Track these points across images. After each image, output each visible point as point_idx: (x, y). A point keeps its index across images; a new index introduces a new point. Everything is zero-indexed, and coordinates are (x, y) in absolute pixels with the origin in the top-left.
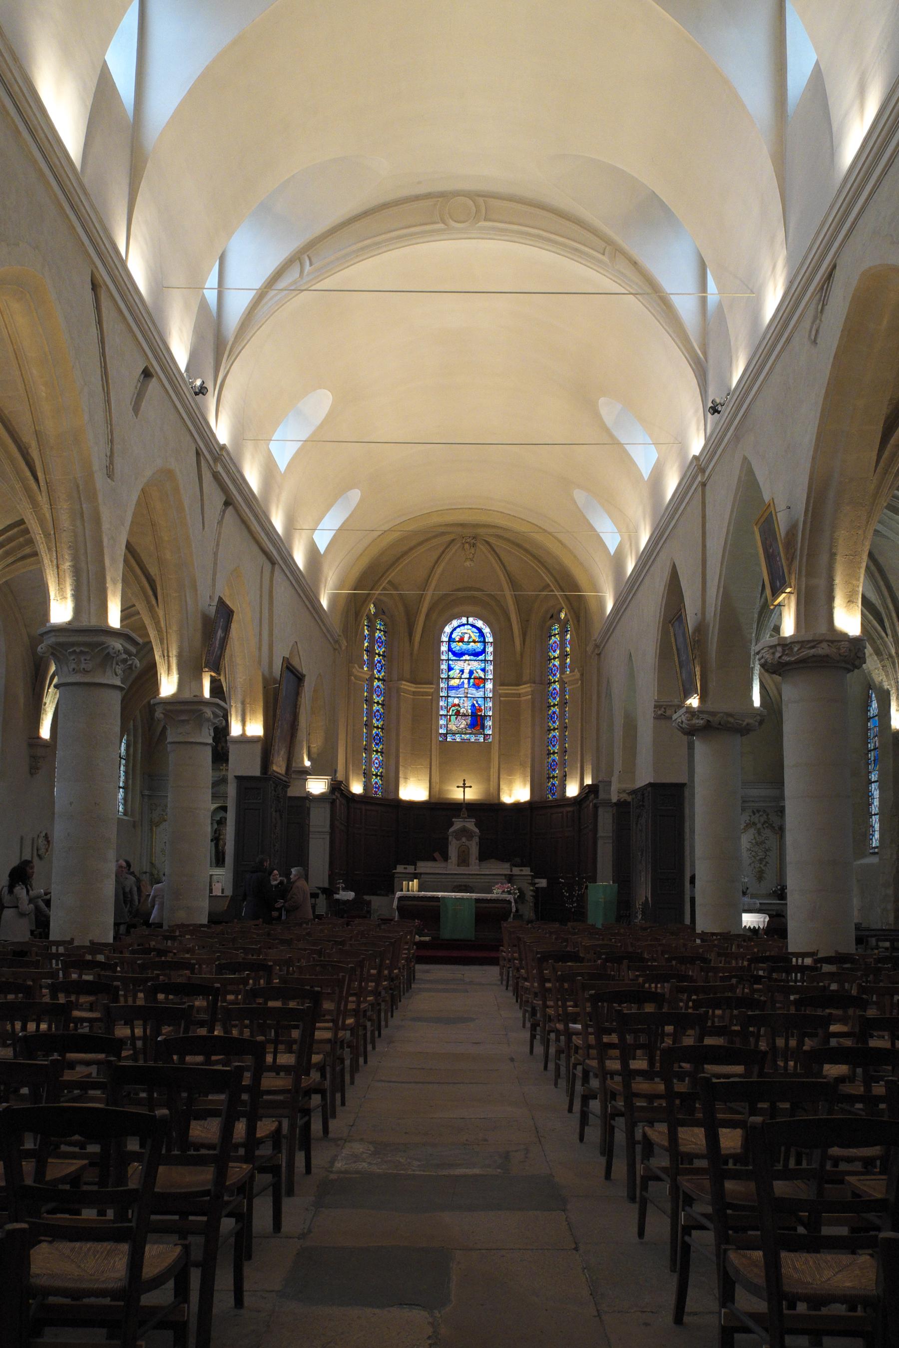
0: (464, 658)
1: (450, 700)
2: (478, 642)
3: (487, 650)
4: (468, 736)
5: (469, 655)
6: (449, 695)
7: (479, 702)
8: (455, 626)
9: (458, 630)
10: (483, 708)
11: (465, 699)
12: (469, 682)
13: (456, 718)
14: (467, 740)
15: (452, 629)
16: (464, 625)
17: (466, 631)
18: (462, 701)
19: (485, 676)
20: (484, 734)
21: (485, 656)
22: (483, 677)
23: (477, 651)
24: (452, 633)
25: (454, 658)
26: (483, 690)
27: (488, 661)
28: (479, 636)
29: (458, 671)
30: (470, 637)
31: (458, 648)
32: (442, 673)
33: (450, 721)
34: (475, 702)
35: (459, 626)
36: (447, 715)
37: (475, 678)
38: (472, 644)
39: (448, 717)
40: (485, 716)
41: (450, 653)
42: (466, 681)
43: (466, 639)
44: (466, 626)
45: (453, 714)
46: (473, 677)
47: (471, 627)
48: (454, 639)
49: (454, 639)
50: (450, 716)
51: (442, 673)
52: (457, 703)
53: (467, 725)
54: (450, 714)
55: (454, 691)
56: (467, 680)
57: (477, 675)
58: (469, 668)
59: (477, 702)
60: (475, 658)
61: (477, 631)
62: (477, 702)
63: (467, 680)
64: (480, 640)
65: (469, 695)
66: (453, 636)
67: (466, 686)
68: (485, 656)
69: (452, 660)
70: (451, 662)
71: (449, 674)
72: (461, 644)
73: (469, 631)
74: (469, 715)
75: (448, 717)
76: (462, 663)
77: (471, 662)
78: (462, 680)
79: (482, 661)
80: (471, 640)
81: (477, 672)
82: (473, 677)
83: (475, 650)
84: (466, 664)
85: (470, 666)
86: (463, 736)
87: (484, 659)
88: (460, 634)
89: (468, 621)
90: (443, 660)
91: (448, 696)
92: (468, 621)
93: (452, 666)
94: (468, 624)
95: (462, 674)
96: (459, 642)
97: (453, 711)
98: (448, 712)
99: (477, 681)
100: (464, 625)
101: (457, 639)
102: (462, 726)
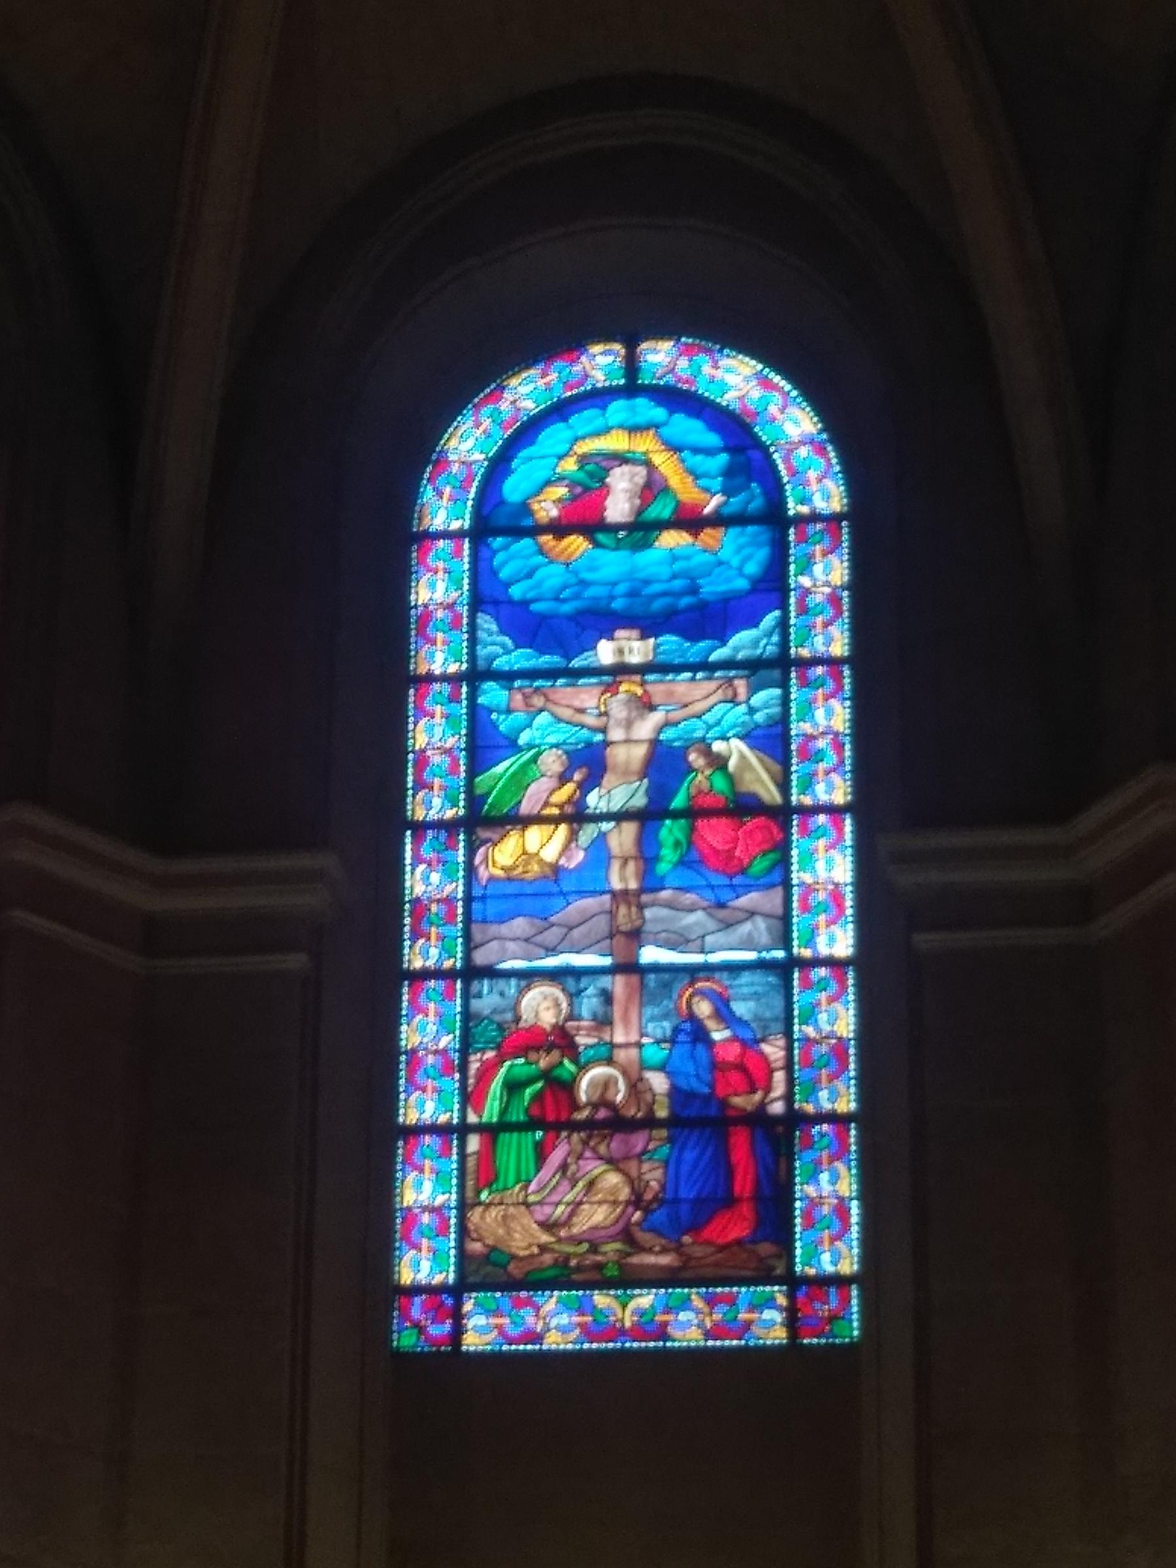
0: (605, 653)
1: (488, 997)
2: (720, 520)
3: (798, 580)
4: (645, 1299)
5: (649, 627)
6: (481, 958)
7: (741, 1008)
8: (530, 406)
9: (554, 437)
10: (773, 1051)
11: (619, 985)
12: (646, 855)
13: (542, 1153)
14: (639, 1332)
15: (500, 437)
16: (599, 397)
17: (617, 442)
18: (589, 1004)
19: (784, 786)
20: (793, 1282)
21: (783, 625)
22: (770, 794)
23: (711, 588)
24: (499, 466)
25: (521, 659)
26: (771, 900)
27: (805, 664)
28: (729, 473)
29: (552, 762)
30: (653, 488)
31: (552, 576)
32: (420, 785)
33: (487, 1173)
34: (703, 1008)
35: (560, 411)
36: (463, 1130)
37: (693, 813)
38: (672, 539)
39: (474, 1143)
40: (796, 1120)
41: (486, 623)
42: (623, 838)
43: (618, 508)
44: (618, 410)
45: (517, 1115)
46: (679, 801)
47: (658, 413)
48: (525, 508)
49: (525, 508)
50: (491, 1132)
51: (420, 785)
52: (548, 1019)
53: (637, 1201)
54: (491, 1110)
55: (520, 925)
56: (630, 829)
57: (720, 783)
58: (646, 728)
59: (723, 1013)
60: (695, 650)
61: (712, 439)
62: (723, 1013)
63: (630, 829)
64: (736, 503)
65: (649, 954)
66: (513, 488)
67: (623, 877)
68: (783, 625)
69: (506, 678)
70: (492, 694)
71: (482, 781)
72: (577, 543)
73: (644, 444)
74: (650, 1122)
75: (474, 1143)
76: (587, 696)
77: (657, 687)
78: (588, 832)
79: (753, 667)
80: (661, 509)
81: (719, 763)
82: (679, 801)
83: (694, 590)
84: (618, 707)
85: (657, 717)
86: (601, 1299)
87: (770, 649)
88: (570, 466)
89: (632, 366)
90: (430, 678)
91: (471, 973)
92: (632, 366)
93: (505, 724)
94: (632, 388)
95: (586, 787)
96: (559, 529)
97: (513, 1087)
98: (471, 1097)
99: (715, 833)
100: (599, 397)
101: (547, 509)
102: (596, 1216)
